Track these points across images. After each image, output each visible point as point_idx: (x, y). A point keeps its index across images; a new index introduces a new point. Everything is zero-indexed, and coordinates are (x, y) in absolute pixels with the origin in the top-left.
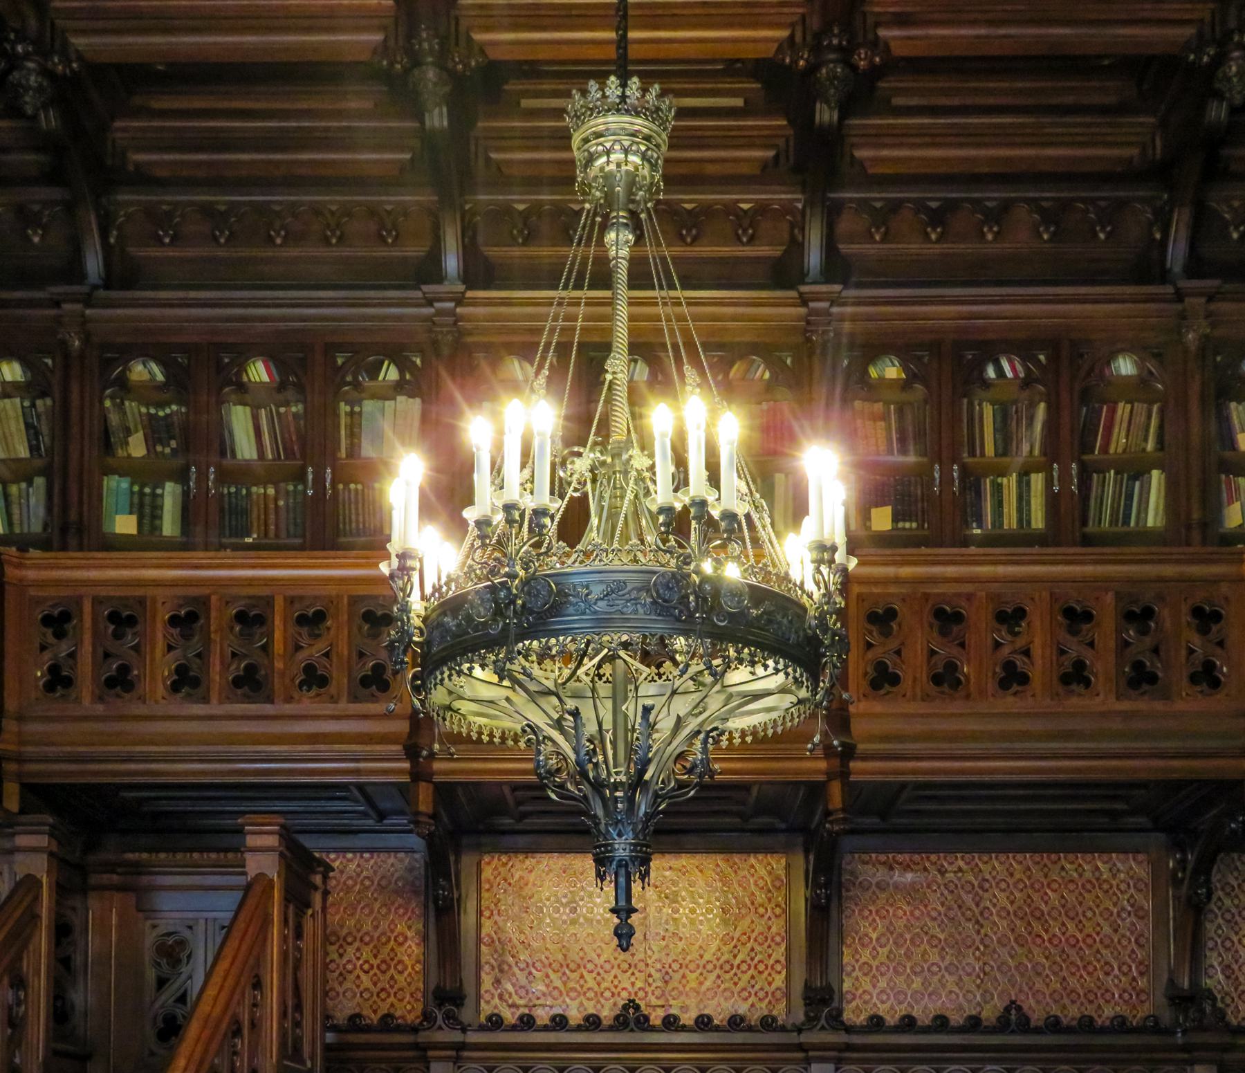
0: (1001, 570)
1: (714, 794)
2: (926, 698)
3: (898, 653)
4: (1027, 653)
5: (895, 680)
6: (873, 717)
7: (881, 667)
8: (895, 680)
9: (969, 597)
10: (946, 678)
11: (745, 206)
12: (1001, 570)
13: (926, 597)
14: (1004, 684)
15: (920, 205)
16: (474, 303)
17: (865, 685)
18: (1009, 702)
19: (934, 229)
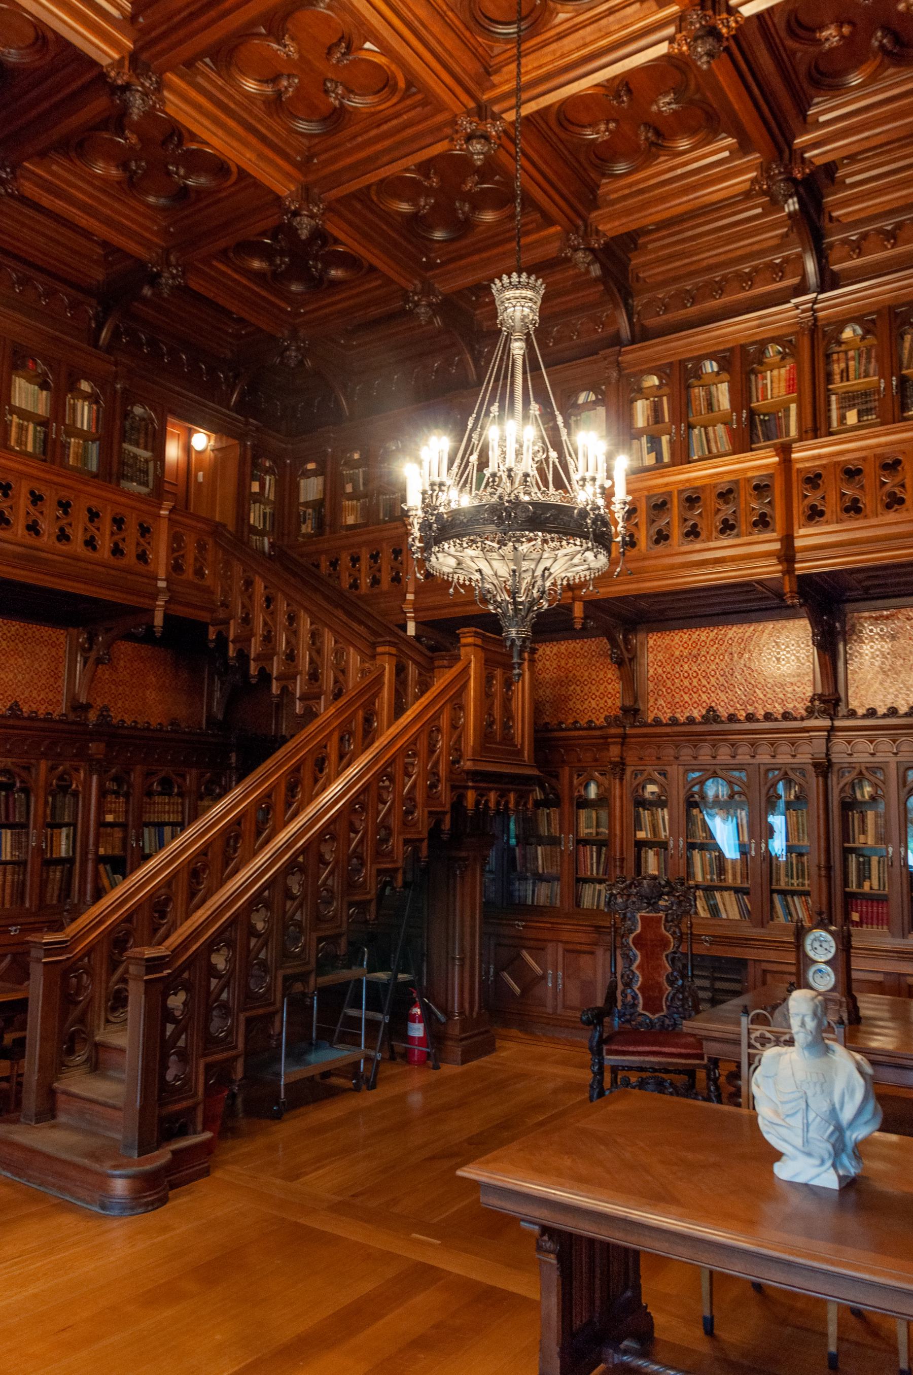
0: (883, 440)
1: (724, 591)
2: (839, 521)
3: (823, 498)
4: (903, 486)
5: (822, 514)
6: (807, 536)
7: (813, 508)
8: (822, 514)
9: (864, 459)
10: (854, 508)
11: (777, 261)
12: (883, 440)
13: (838, 463)
14: (889, 506)
15: (880, 231)
16: (627, 353)
17: (802, 518)
18: (891, 517)
19: (888, 241)
